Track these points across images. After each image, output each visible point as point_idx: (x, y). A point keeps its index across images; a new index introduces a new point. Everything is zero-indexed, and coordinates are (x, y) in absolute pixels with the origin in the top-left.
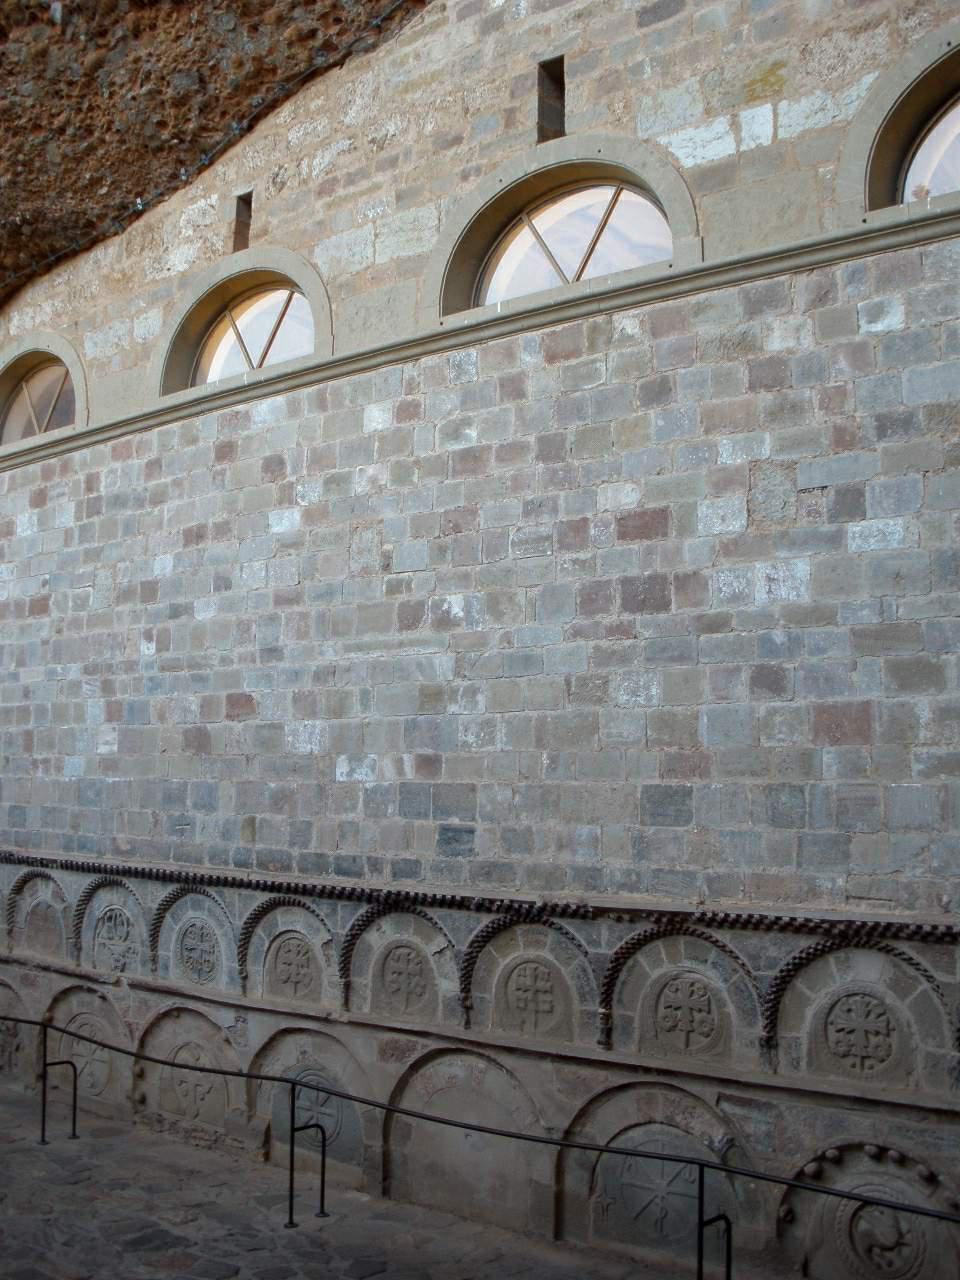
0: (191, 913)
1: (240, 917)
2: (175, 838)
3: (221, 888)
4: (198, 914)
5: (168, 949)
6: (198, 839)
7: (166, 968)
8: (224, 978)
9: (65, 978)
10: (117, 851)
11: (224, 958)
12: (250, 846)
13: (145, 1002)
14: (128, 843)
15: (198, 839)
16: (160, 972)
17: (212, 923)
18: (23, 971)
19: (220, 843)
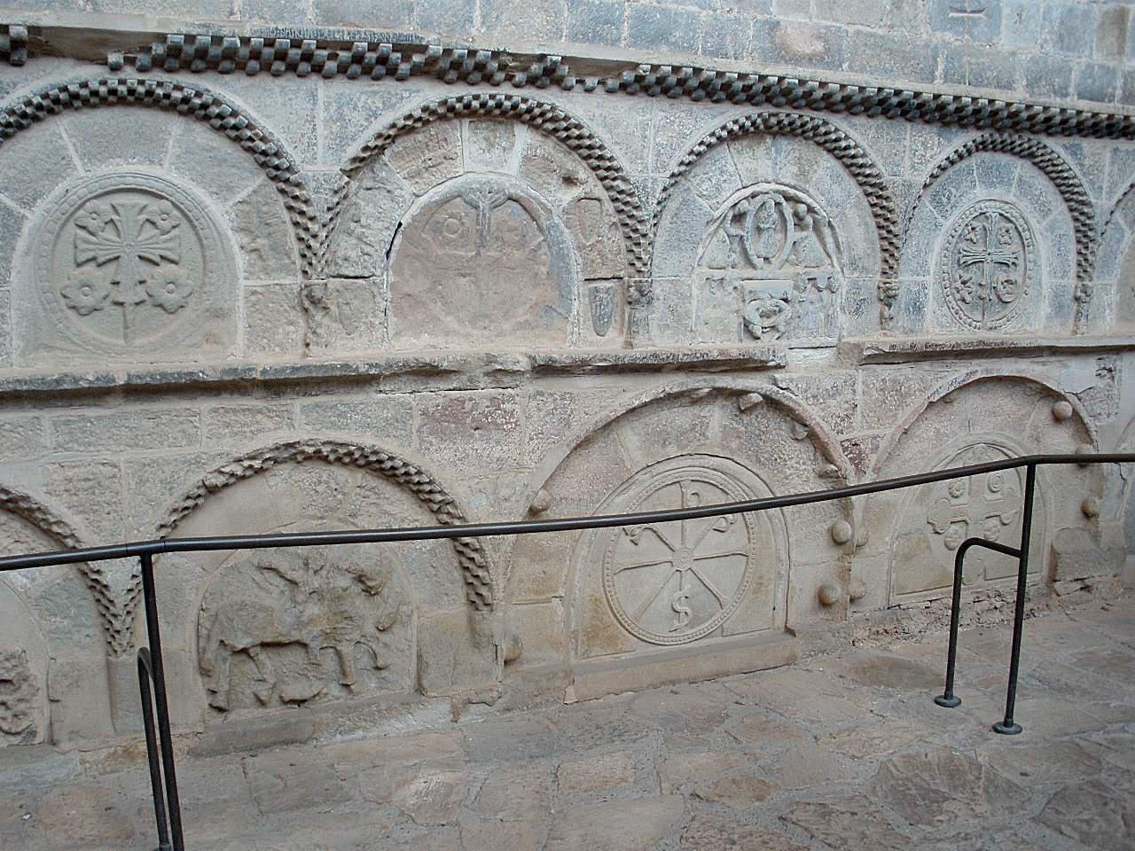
0: (980, 192)
1: (1111, 192)
2: (949, 36)
3: (1076, 140)
4: (997, 192)
5: (923, 268)
6: (1005, 42)
7: (917, 308)
8: (1045, 309)
9: (627, 382)
10: (782, 53)
11: (1045, 270)
12: (1112, 64)
13: (896, 387)
14: (819, 37)
15: (1005, 42)
16: (903, 320)
17: (1024, 206)
18: (435, 395)
19: (1054, 54)
